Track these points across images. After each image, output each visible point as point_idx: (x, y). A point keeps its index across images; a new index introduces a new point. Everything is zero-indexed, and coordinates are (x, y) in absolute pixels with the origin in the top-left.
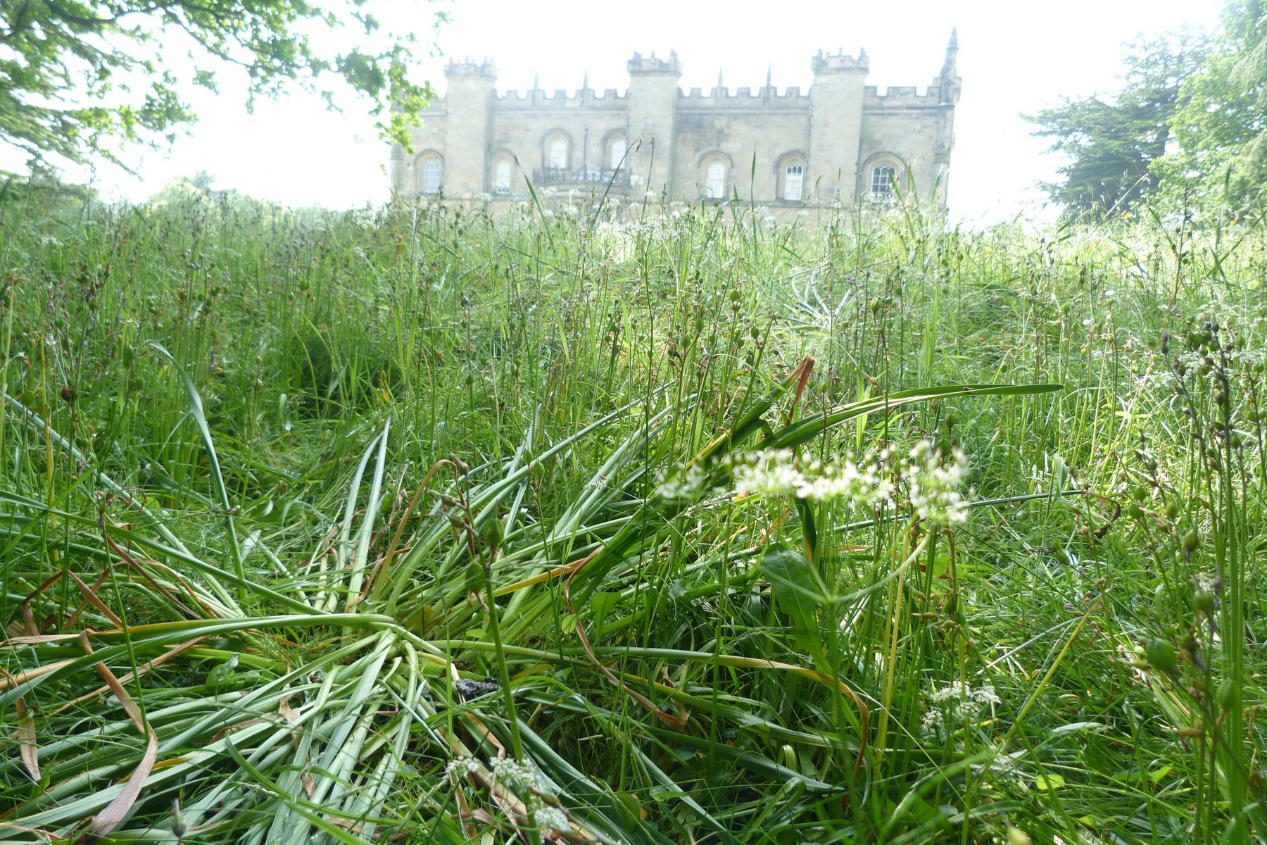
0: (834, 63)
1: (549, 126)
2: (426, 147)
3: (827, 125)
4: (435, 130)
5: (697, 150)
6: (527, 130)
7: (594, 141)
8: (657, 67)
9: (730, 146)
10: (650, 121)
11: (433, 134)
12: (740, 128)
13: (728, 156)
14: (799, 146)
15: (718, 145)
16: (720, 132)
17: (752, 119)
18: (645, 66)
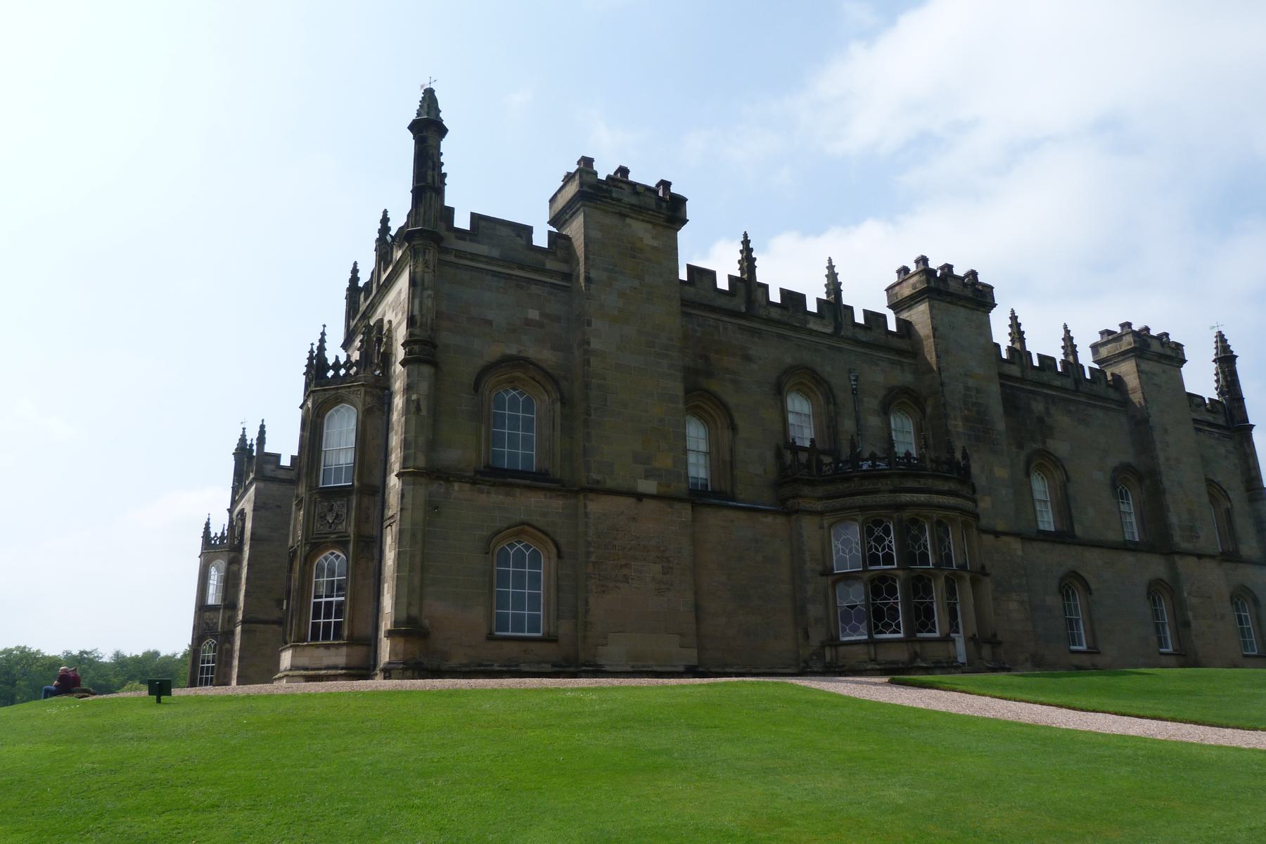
0: (1156, 347)
1: (788, 360)
2: (512, 350)
3: (1166, 431)
4: (534, 314)
5: (1020, 446)
6: (747, 358)
7: (871, 403)
8: (968, 292)
9: (1059, 447)
10: (971, 382)
11: (528, 322)
12: (1061, 420)
13: (1057, 463)
14: (1128, 457)
15: (1044, 443)
16: (1041, 420)
17: (1073, 408)
18: (953, 287)
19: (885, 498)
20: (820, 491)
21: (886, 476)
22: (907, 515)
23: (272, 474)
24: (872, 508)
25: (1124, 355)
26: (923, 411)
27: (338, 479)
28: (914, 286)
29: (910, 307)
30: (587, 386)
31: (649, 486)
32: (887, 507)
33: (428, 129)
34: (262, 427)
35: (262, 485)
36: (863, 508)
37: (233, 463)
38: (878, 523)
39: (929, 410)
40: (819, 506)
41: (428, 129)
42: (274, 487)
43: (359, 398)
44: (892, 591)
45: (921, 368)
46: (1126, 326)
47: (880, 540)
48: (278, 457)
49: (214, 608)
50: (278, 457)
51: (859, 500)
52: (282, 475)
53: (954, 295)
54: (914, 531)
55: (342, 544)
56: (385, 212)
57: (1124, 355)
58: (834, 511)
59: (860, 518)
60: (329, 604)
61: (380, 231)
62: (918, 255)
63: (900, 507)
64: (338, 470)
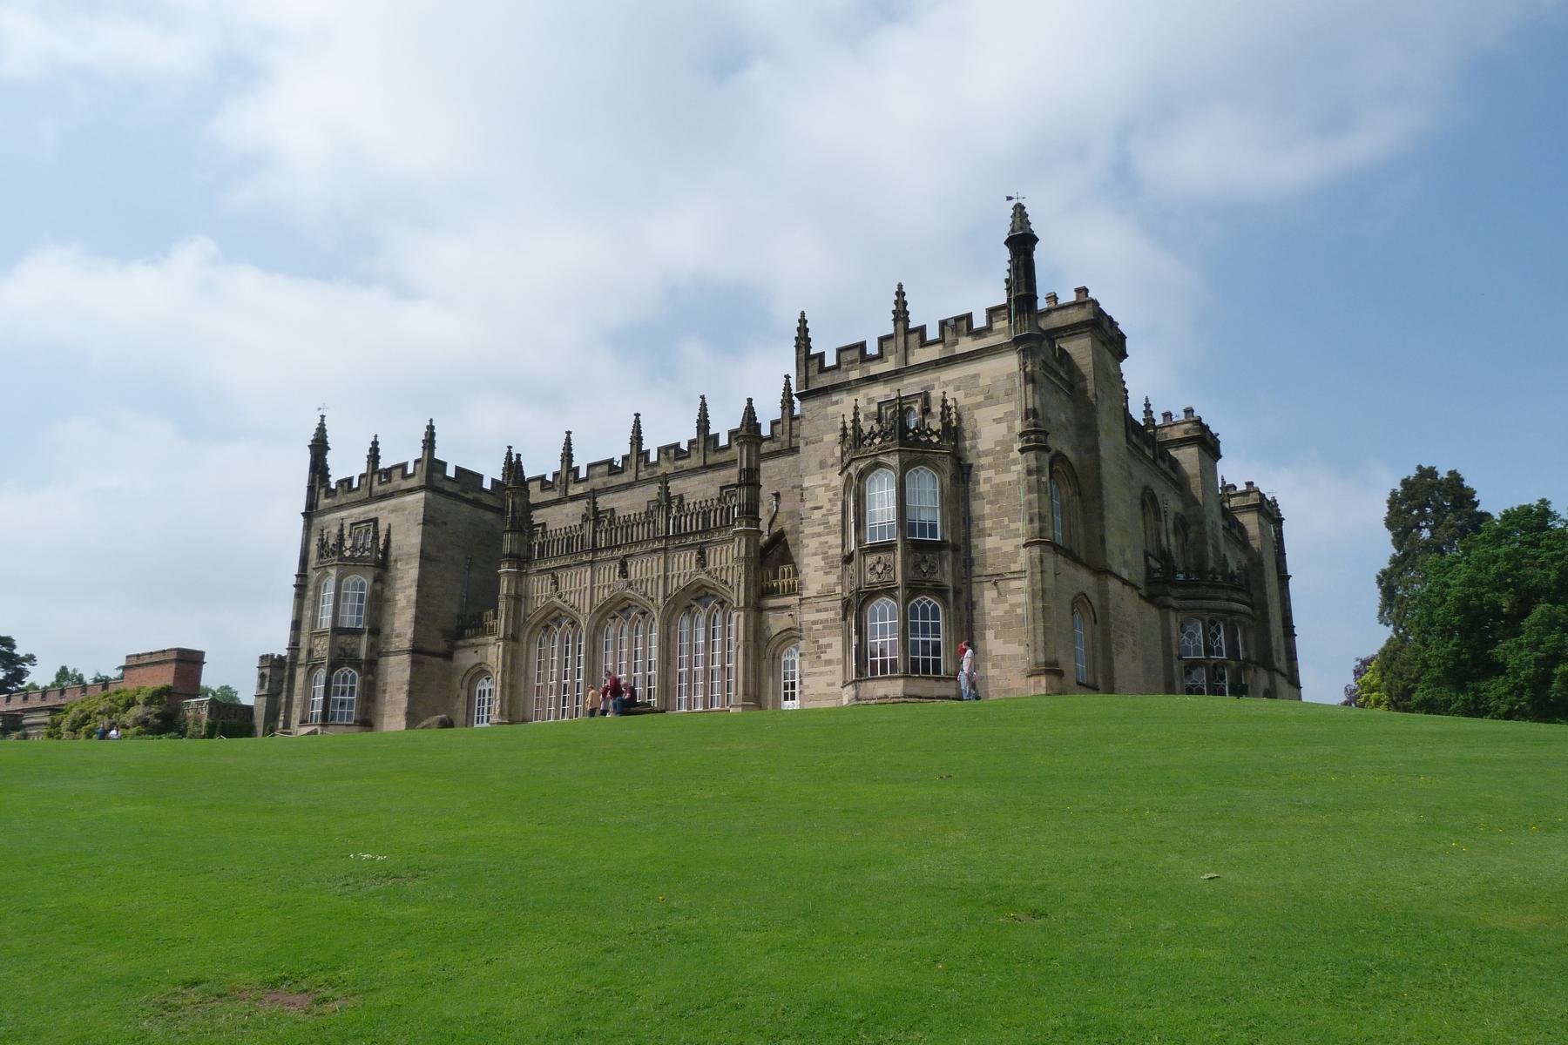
11: (1063, 425)
19: (1221, 604)
20: (1175, 592)
21: (1223, 587)
22: (1236, 618)
23: (438, 484)
24: (1214, 610)
25: (1249, 508)
26: (1186, 535)
27: (923, 534)
28: (1186, 431)
29: (1177, 447)
30: (1100, 486)
31: (1125, 574)
32: (1222, 611)
33: (1022, 243)
34: (431, 428)
35: (430, 495)
36: (1209, 610)
37: (308, 457)
38: (1212, 622)
39: (1192, 536)
40: (1175, 604)
41: (1022, 243)
42: (441, 499)
43: (947, 465)
44: (1222, 677)
45: (1189, 500)
46: (1250, 484)
47: (1214, 636)
48: (444, 464)
49: (356, 632)
50: (444, 464)
51: (1205, 603)
52: (448, 487)
53: (1208, 444)
54: (1213, 630)
55: (939, 591)
56: (900, 286)
57: (1249, 508)
58: (1185, 610)
59: (1207, 618)
60: (925, 643)
61: (896, 303)
62: (1188, 405)
63: (1232, 612)
64: (923, 526)
